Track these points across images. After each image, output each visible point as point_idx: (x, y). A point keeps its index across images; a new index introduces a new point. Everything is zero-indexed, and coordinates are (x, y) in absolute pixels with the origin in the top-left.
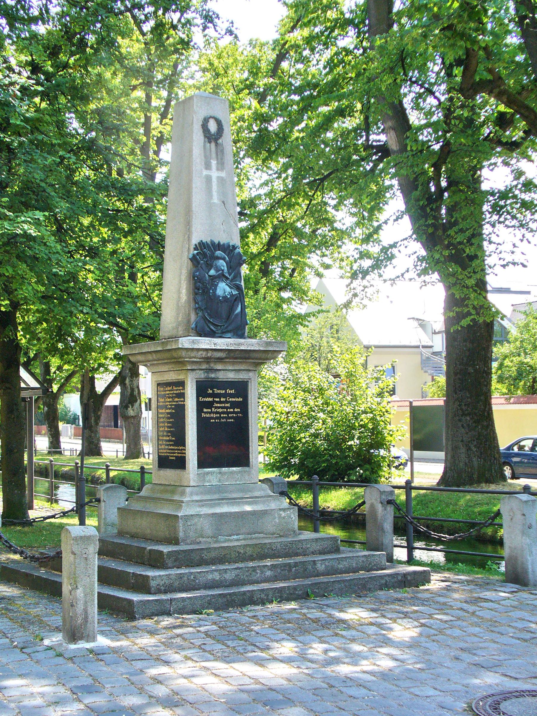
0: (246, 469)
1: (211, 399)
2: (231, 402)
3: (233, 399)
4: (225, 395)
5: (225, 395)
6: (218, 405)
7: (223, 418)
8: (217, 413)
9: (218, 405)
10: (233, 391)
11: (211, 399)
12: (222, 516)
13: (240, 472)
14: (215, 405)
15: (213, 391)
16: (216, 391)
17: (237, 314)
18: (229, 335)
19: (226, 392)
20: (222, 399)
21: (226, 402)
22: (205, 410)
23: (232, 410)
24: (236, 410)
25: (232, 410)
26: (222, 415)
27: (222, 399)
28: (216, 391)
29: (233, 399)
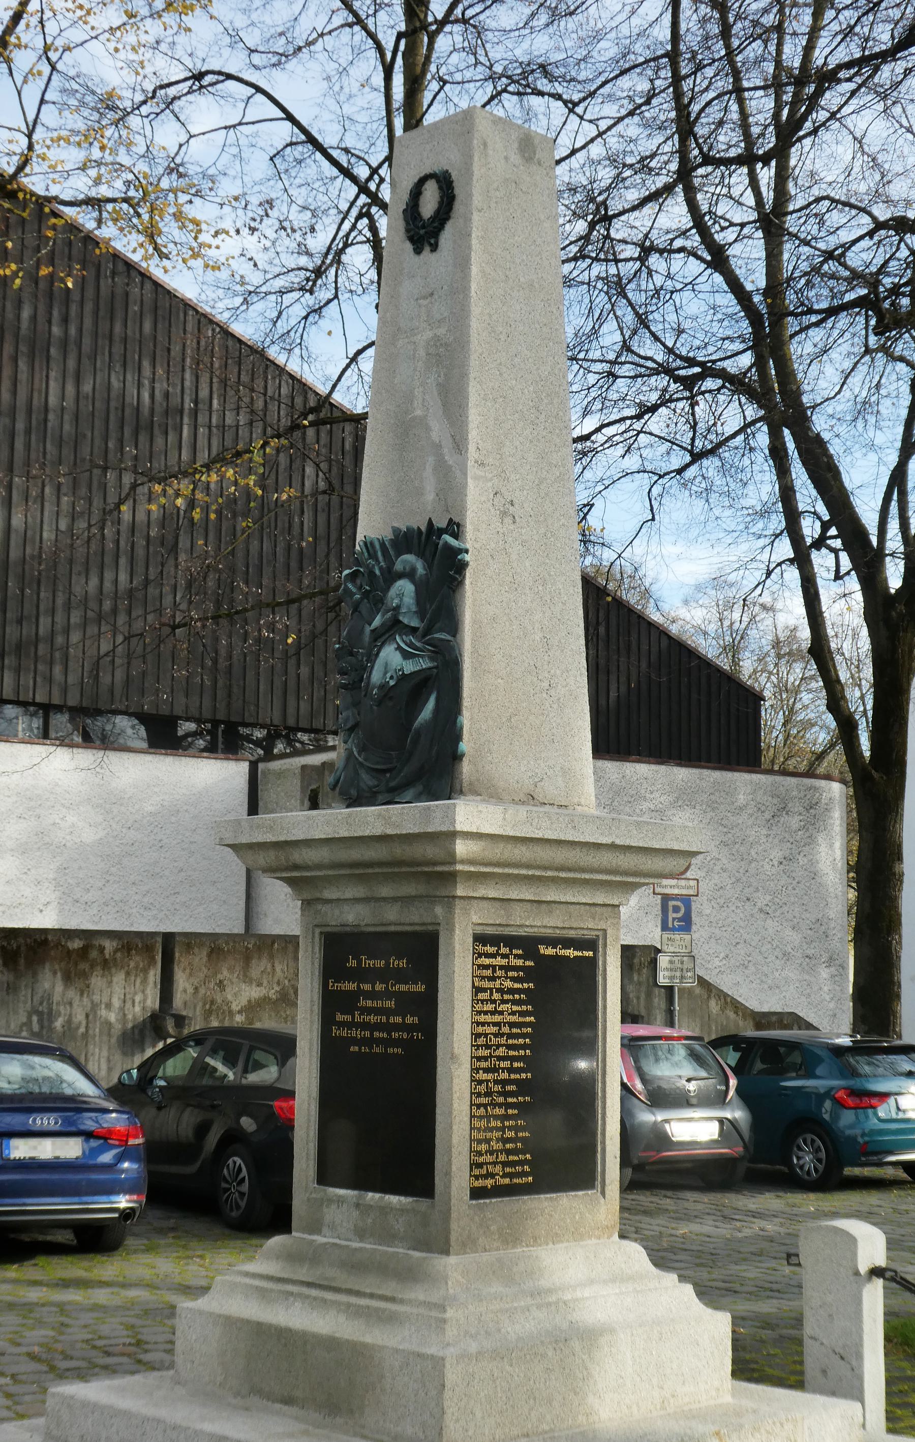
0: (423, 1204)
1: (352, 986)
2: (399, 995)
3: (403, 988)
4: (383, 975)
5: (383, 975)
6: (369, 1003)
7: (379, 1041)
8: (364, 1026)
9: (369, 1003)
10: (403, 963)
11: (352, 986)
12: (283, 1335)
13: (402, 1211)
14: (362, 1003)
15: (360, 962)
16: (368, 963)
17: (418, 733)
18: (410, 794)
19: (388, 963)
20: (379, 987)
21: (387, 994)
22: (340, 1017)
23: (399, 1020)
24: (409, 1020)
25: (399, 1020)
26: (376, 1034)
27: (379, 987)
28: (368, 963)
29: (403, 988)
